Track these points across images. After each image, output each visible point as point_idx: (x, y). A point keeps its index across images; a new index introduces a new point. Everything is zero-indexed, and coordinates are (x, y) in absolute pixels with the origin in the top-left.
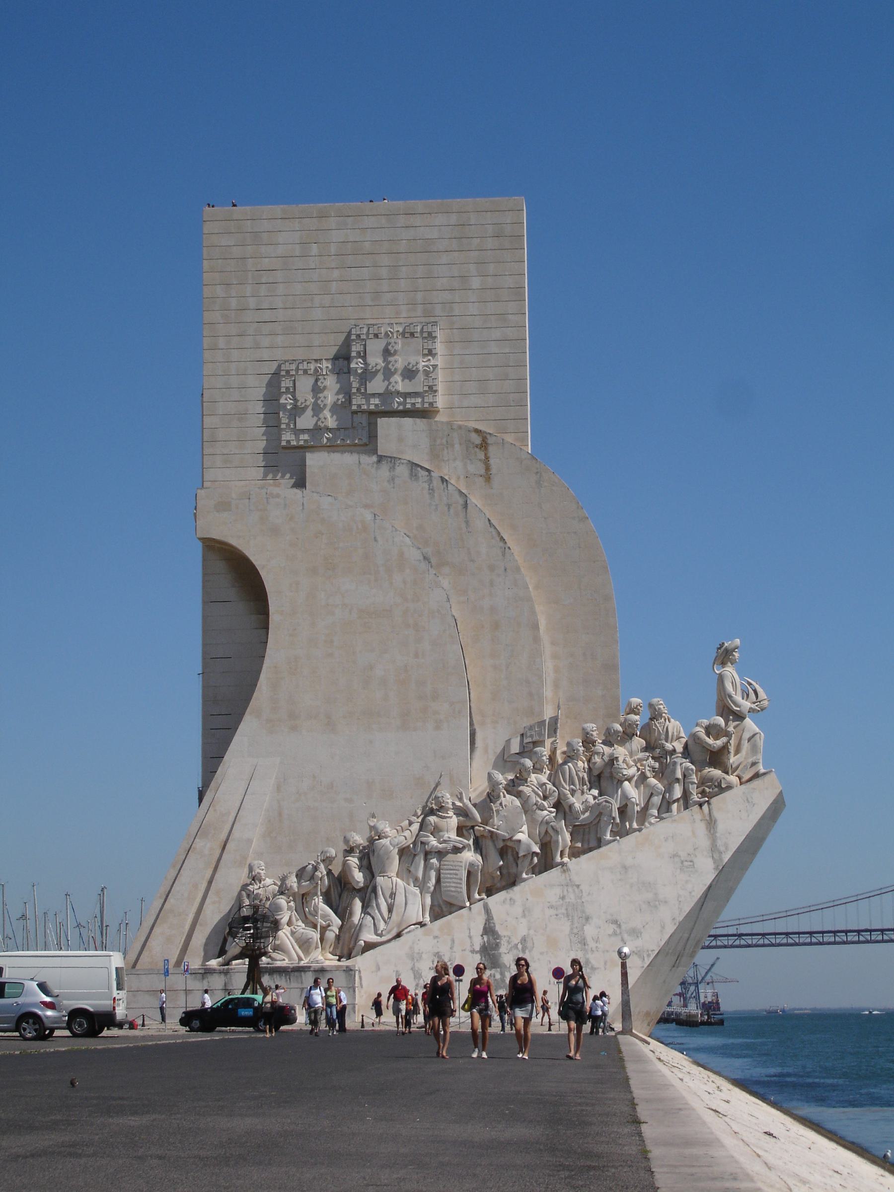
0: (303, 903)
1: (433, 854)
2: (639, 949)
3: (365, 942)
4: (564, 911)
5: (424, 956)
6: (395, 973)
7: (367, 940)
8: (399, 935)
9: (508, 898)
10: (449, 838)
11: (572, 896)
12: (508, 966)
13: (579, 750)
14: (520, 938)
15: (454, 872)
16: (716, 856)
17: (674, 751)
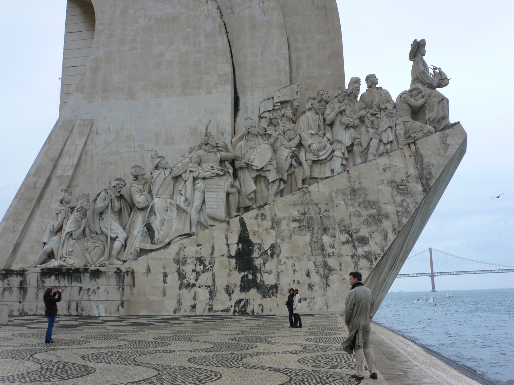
0: (100, 220)
1: (200, 180)
2: (367, 253)
3: (141, 249)
4: (305, 224)
5: (189, 261)
6: (163, 274)
7: (142, 248)
8: (169, 243)
9: (260, 215)
10: (212, 167)
11: (312, 212)
12: (259, 268)
13: (316, 105)
14: (269, 245)
15: (217, 193)
16: (424, 181)
17: (386, 108)
